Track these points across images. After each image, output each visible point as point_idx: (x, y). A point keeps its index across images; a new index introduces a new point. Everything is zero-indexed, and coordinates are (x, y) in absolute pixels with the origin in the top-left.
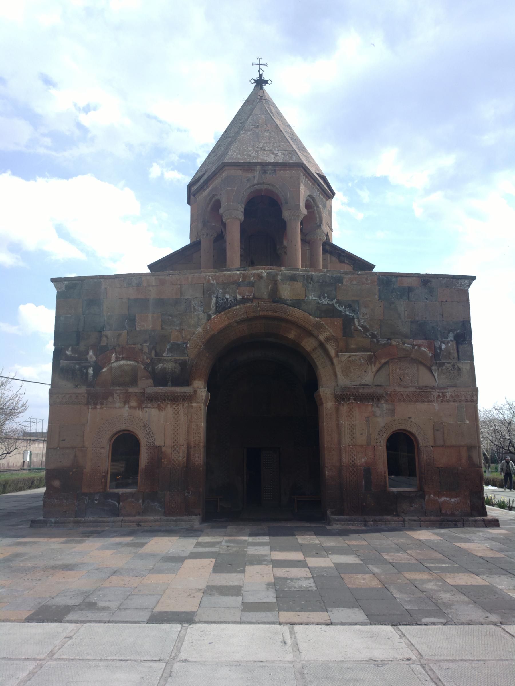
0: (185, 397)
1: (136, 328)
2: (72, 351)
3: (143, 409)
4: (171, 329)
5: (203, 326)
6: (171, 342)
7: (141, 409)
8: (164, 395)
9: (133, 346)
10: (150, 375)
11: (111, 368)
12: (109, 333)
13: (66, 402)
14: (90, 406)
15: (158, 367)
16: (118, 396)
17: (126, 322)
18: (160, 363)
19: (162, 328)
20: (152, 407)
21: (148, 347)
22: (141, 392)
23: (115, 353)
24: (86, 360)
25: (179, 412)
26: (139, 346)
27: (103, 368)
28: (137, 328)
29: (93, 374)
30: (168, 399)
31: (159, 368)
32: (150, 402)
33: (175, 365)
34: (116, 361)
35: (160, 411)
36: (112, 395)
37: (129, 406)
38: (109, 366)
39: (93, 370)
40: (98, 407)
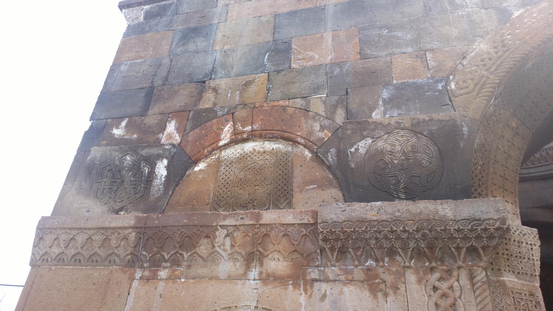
0: (479, 237)
1: (290, 66)
2: (127, 126)
3: (312, 286)
4: (390, 54)
5: (489, 37)
6: (395, 82)
7: (305, 284)
8: (392, 231)
9: (281, 103)
10: (331, 176)
11: (219, 160)
12: (222, 82)
13: (74, 256)
14: (138, 270)
15: (357, 150)
16: (227, 235)
17: (266, 57)
18: (363, 138)
19: (363, 57)
20: (343, 278)
21: (324, 102)
22: (306, 221)
23: (232, 123)
24: (158, 143)
25: (459, 303)
26: (299, 102)
27: (196, 162)
28: (294, 66)
29: (166, 177)
30: (405, 249)
31: (362, 151)
32: (338, 260)
33: (415, 139)
34: (234, 142)
35: (375, 296)
36: (210, 236)
37: (261, 273)
38: (213, 157)
39: (168, 168)
40: (163, 274)
